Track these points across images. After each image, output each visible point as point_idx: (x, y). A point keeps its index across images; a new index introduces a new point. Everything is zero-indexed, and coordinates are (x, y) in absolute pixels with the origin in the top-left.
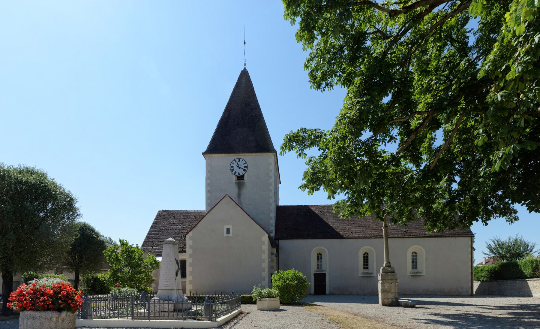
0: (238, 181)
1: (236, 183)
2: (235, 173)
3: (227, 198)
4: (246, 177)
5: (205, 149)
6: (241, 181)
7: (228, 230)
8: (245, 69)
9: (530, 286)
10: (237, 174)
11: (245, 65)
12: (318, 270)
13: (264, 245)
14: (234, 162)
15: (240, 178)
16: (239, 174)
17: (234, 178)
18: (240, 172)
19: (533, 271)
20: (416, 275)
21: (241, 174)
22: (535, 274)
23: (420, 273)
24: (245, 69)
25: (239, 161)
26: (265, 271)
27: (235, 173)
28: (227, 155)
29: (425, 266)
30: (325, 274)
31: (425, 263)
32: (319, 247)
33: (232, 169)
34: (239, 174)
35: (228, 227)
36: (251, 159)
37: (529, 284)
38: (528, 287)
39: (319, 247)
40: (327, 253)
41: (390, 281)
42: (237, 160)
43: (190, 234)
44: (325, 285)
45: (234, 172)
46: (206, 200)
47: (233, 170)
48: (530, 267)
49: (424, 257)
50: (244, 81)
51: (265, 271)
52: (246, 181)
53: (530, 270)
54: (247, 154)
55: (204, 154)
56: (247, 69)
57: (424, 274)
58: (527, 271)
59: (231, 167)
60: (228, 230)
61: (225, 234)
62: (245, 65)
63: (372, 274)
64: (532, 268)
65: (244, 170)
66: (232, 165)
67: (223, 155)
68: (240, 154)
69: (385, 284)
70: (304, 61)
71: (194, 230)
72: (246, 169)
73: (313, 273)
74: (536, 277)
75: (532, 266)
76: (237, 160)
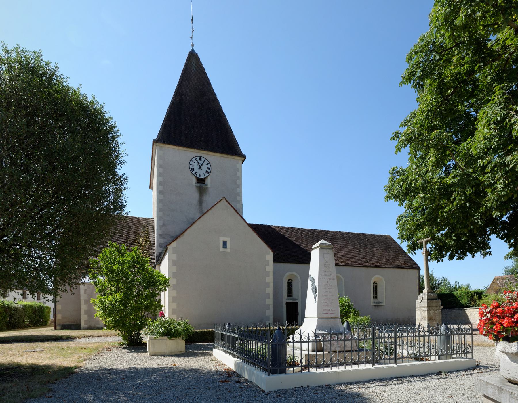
0: (198, 185)
1: (196, 186)
2: (196, 173)
3: (224, 202)
4: (208, 181)
5: (155, 136)
6: (203, 185)
7: (225, 244)
8: (193, 49)
9: (468, 315)
10: (198, 176)
11: (193, 45)
12: (290, 298)
13: (268, 265)
14: (194, 160)
15: (201, 181)
16: (200, 175)
17: (194, 180)
18: (202, 173)
19: (468, 301)
20: (378, 305)
21: (203, 177)
22: (470, 304)
23: (381, 303)
24: (193, 49)
25: (201, 159)
26: (269, 298)
27: (196, 173)
28: (185, 149)
29: (384, 295)
30: (297, 303)
31: (384, 293)
32: (291, 273)
33: (191, 167)
34: (200, 175)
35: (225, 239)
36: (215, 159)
37: (467, 313)
38: (466, 315)
39: (291, 273)
40: (300, 280)
41: (435, 308)
42: (198, 158)
43: (174, 244)
44: (298, 315)
45: (194, 173)
46: (158, 203)
47: (193, 169)
48: (466, 298)
49: (384, 287)
50: (194, 64)
51: (269, 298)
52: (209, 186)
53: (466, 300)
54: (211, 153)
55: (155, 141)
56: (197, 51)
57: (384, 304)
58: (464, 301)
59: (190, 165)
60: (225, 243)
61: (221, 249)
62: (193, 45)
63: (381, 303)
64: (468, 299)
65: (207, 172)
66: (192, 163)
67: (181, 148)
68: (202, 152)
69: (431, 312)
70: (408, 53)
71: (179, 239)
72: (209, 171)
73: (285, 302)
74: (470, 307)
75: (468, 297)
76: (198, 158)
